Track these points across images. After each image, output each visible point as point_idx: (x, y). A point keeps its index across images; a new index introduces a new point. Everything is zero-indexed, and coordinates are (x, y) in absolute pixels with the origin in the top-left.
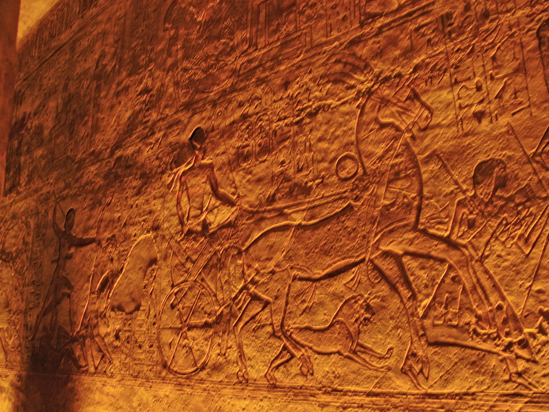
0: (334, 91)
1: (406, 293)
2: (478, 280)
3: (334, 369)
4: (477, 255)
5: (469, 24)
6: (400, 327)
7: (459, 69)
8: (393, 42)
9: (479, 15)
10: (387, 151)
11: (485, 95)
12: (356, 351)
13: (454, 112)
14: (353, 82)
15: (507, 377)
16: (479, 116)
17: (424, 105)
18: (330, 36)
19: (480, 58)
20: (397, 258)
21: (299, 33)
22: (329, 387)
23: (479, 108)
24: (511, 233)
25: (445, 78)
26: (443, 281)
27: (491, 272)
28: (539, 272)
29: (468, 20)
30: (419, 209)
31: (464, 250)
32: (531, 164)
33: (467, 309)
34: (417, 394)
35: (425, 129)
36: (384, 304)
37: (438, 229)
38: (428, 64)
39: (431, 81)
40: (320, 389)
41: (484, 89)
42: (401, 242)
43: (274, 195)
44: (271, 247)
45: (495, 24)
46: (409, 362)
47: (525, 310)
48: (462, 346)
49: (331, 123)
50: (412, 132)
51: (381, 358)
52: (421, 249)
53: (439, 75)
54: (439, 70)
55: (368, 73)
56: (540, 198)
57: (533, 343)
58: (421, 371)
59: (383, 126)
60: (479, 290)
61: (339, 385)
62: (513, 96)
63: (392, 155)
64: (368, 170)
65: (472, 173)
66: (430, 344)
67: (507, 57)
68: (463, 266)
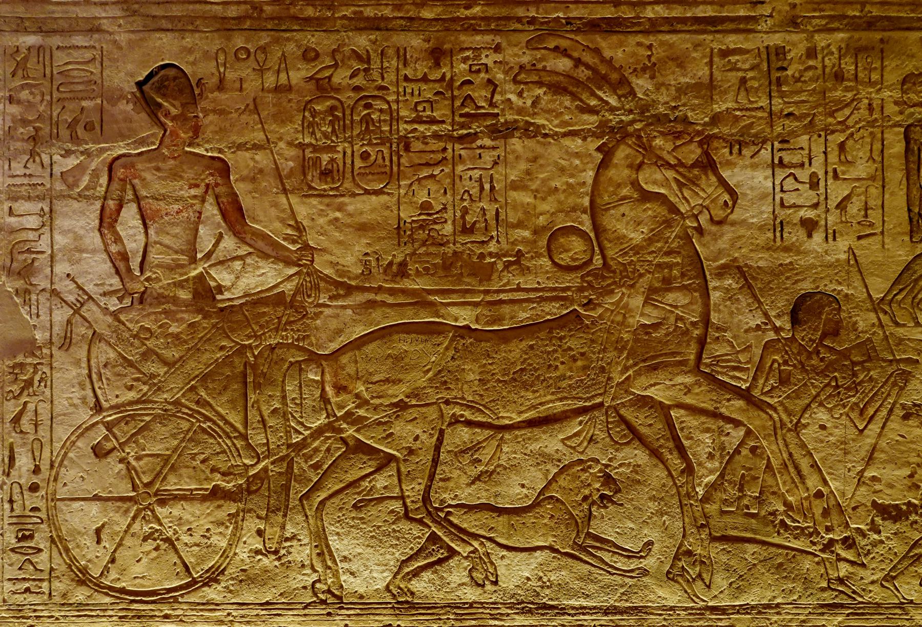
1: (675, 462)
2: (791, 455)
3: (541, 574)
4: (791, 422)
6: (666, 514)
7: (786, 146)
8: (680, 61)
10: (650, 241)
11: (822, 198)
12: (585, 546)
14: (593, 102)
15: (824, 584)
16: (809, 226)
17: (723, 182)
19: (822, 140)
20: (663, 410)
22: (532, 603)
24: (842, 400)
25: (763, 151)
26: (737, 451)
28: (875, 455)
30: (702, 343)
31: (771, 412)
32: (877, 313)
33: (774, 493)
34: (692, 608)
35: (720, 223)
36: (638, 477)
37: (732, 377)
38: (737, 119)
39: (740, 150)
40: (511, 606)
41: (822, 190)
43: (403, 265)
44: (398, 359)
45: (850, 95)
46: (680, 564)
47: (853, 501)
49: (542, 162)
51: (631, 555)
53: (754, 144)
58: (699, 575)
59: (646, 196)
60: (792, 470)
63: (660, 249)
66: (714, 539)
67: (861, 154)
68: (770, 435)
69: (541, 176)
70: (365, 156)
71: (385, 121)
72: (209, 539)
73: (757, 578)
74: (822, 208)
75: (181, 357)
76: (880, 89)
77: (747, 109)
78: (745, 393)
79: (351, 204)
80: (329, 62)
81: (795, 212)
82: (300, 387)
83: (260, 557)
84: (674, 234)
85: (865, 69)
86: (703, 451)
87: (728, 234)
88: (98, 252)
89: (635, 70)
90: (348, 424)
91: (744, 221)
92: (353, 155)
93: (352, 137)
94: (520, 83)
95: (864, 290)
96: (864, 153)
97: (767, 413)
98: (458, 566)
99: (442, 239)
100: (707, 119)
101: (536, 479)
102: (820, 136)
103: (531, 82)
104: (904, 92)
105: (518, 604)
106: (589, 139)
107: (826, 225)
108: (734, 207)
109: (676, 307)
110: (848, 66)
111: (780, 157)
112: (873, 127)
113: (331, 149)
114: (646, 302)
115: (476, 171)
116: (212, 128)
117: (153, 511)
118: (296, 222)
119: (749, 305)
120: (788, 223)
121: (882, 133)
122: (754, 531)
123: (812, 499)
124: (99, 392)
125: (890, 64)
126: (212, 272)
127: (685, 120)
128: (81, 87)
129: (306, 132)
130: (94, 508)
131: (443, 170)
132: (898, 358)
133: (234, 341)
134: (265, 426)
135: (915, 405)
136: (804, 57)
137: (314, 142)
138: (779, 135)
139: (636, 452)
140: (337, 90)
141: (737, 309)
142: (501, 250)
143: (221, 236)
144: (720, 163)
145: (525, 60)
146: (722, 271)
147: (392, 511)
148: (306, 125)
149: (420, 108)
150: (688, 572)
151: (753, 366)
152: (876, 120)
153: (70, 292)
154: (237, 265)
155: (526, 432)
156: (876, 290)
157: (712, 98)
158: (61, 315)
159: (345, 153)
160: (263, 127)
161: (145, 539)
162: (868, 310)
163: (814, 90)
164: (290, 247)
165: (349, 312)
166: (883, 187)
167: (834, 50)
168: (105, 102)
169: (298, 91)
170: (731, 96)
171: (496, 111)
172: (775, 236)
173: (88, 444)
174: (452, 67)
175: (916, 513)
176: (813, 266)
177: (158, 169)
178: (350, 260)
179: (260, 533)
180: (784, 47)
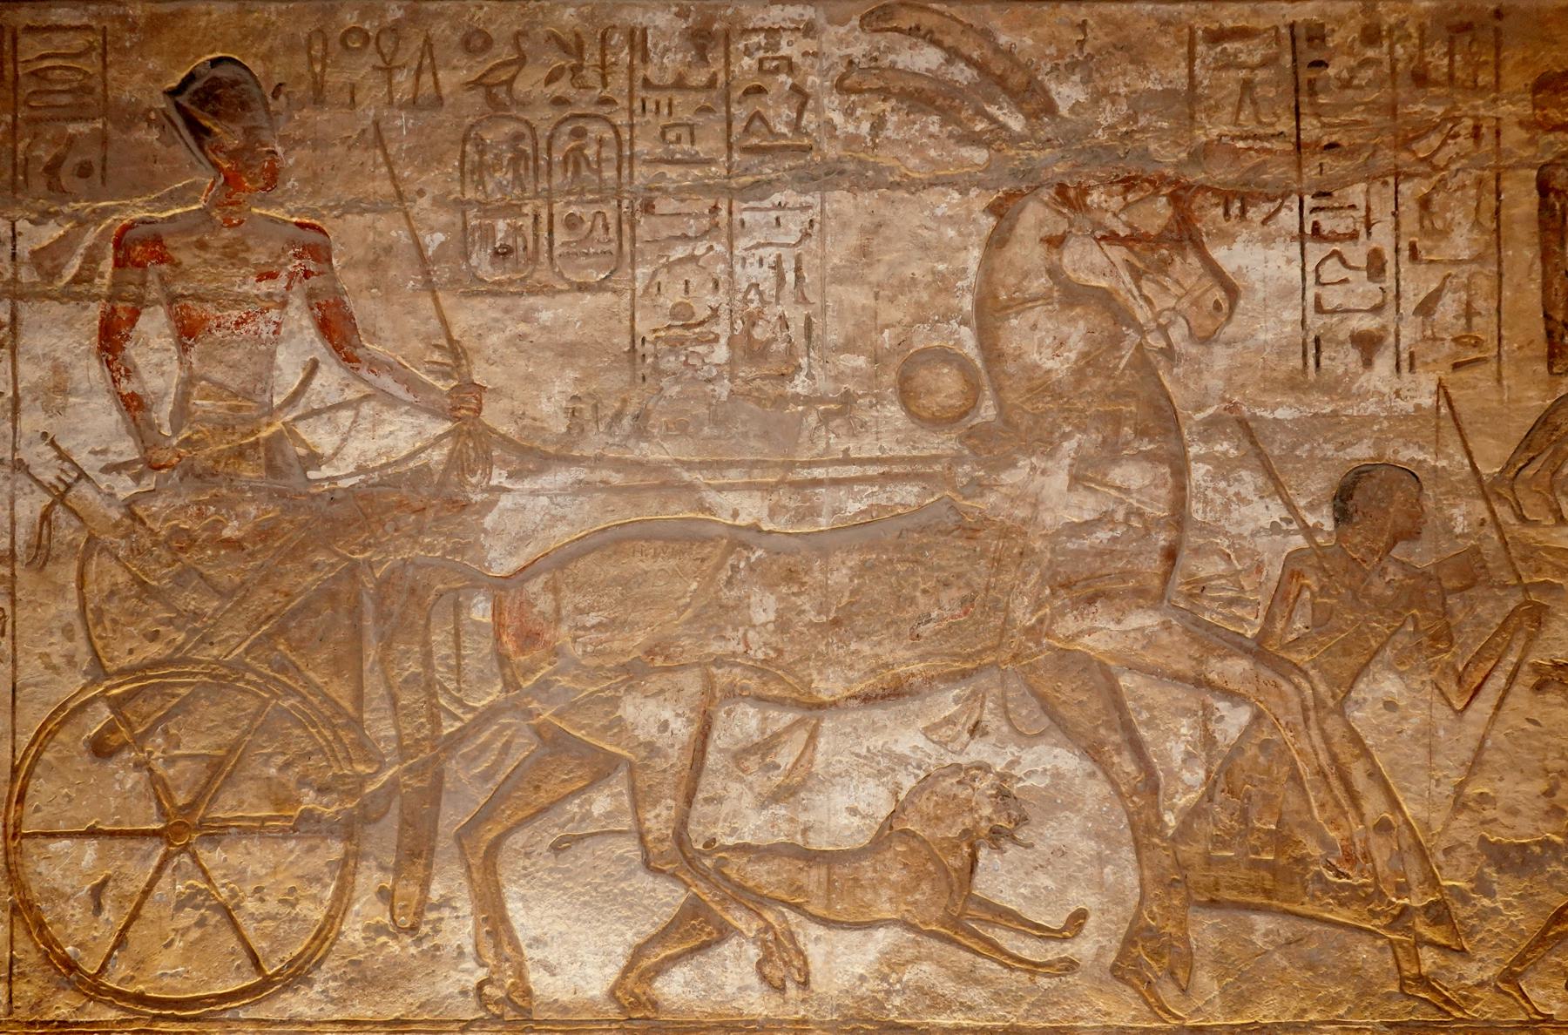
2: (1334, 758)
3: (886, 970)
7: (1324, 202)
11: (1391, 296)
13: (1298, 316)
16: (1367, 344)
23: (1368, 323)
25: (1284, 212)
26: (1238, 748)
27: (1369, 742)
28: (1486, 756)
29: (1370, 73)
32: (1487, 500)
33: (1302, 825)
38: (1237, 153)
39: (1243, 211)
46: (1138, 951)
48: (1286, 912)
50: (1167, 339)
51: (1045, 934)
57: (1461, 911)
60: (1335, 782)
61: (904, 1015)
70: (572, 223)
71: (608, 160)
72: (293, 906)
73: (1273, 977)
74: (1390, 312)
75: (243, 583)
76: (1495, 101)
77: (1255, 137)
79: (547, 309)
80: (505, 53)
81: (1342, 321)
82: (457, 635)
83: (383, 939)
84: (1124, 362)
86: (1177, 750)
87: (1221, 358)
88: (96, 393)
89: (1056, 67)
90: (540, 702)
92: (551, 222)
93: (549, 190)
94: (850, 91)
95: (1466, 461)
96: (1466, 216)
97: (1290, 681)
98: (738, 958)
99: (710, 371)
101: (876, 800)
102: (1385, 183)
103: (870, 90)
105: (844, 1023)
106: (973, 192)
107: (1397, 346)
108: (1232, 308)
109: (1127, 491)
110: (1437, 59)
111: (1315, 223)
113: (512, 209)
115: (770, 250)
116: (300, 172)
117: (194, 856)
118: (450, 339)
119: (1256, 489)
121: (1498, 179)
122: (1268, 893)
123: (1371, 835)
124: (99, 644)
125: (1512, 55)
126: (301, 429)
128: (65, 99)
129: (468, 180)
130: (90, 851)
131: (711, 248)
133: (337, 554)
134: (394, 704)
135: (1557, 666)
136: (1357, 45)
137: (480, 196)
139: (1057, 751)
140: (523, 104)
142: (815, 391)
143: (313, 367)
144: (1208, 234)
145: (858, 51)
146: (1212, 428)
147: (621, 858)
148: (467, 166)
149: (671, 136)
150: (1150, 968)
153: (46, 465)
154: (345, 416)
155: (862, 716)
157: (1192, 117)
158: (30, 506)
159: (536, 217)
160: (391, 170)
161: (180, 906)
162: (1472, 497)
163: (1373, 102)
164: (439, 384)
165: (544, 500)
167: (1412, 30)
168: (110, 127)
169: (453, 105)
171: (806, 141)
172: (1305, 364)
173: (79, 738)
174: (728, 63)
175: (1558, 860)
176: (1374, 418)
177: (202, 245)
178: (549, 408)
179: (385, 895)
180: (1322, 26)
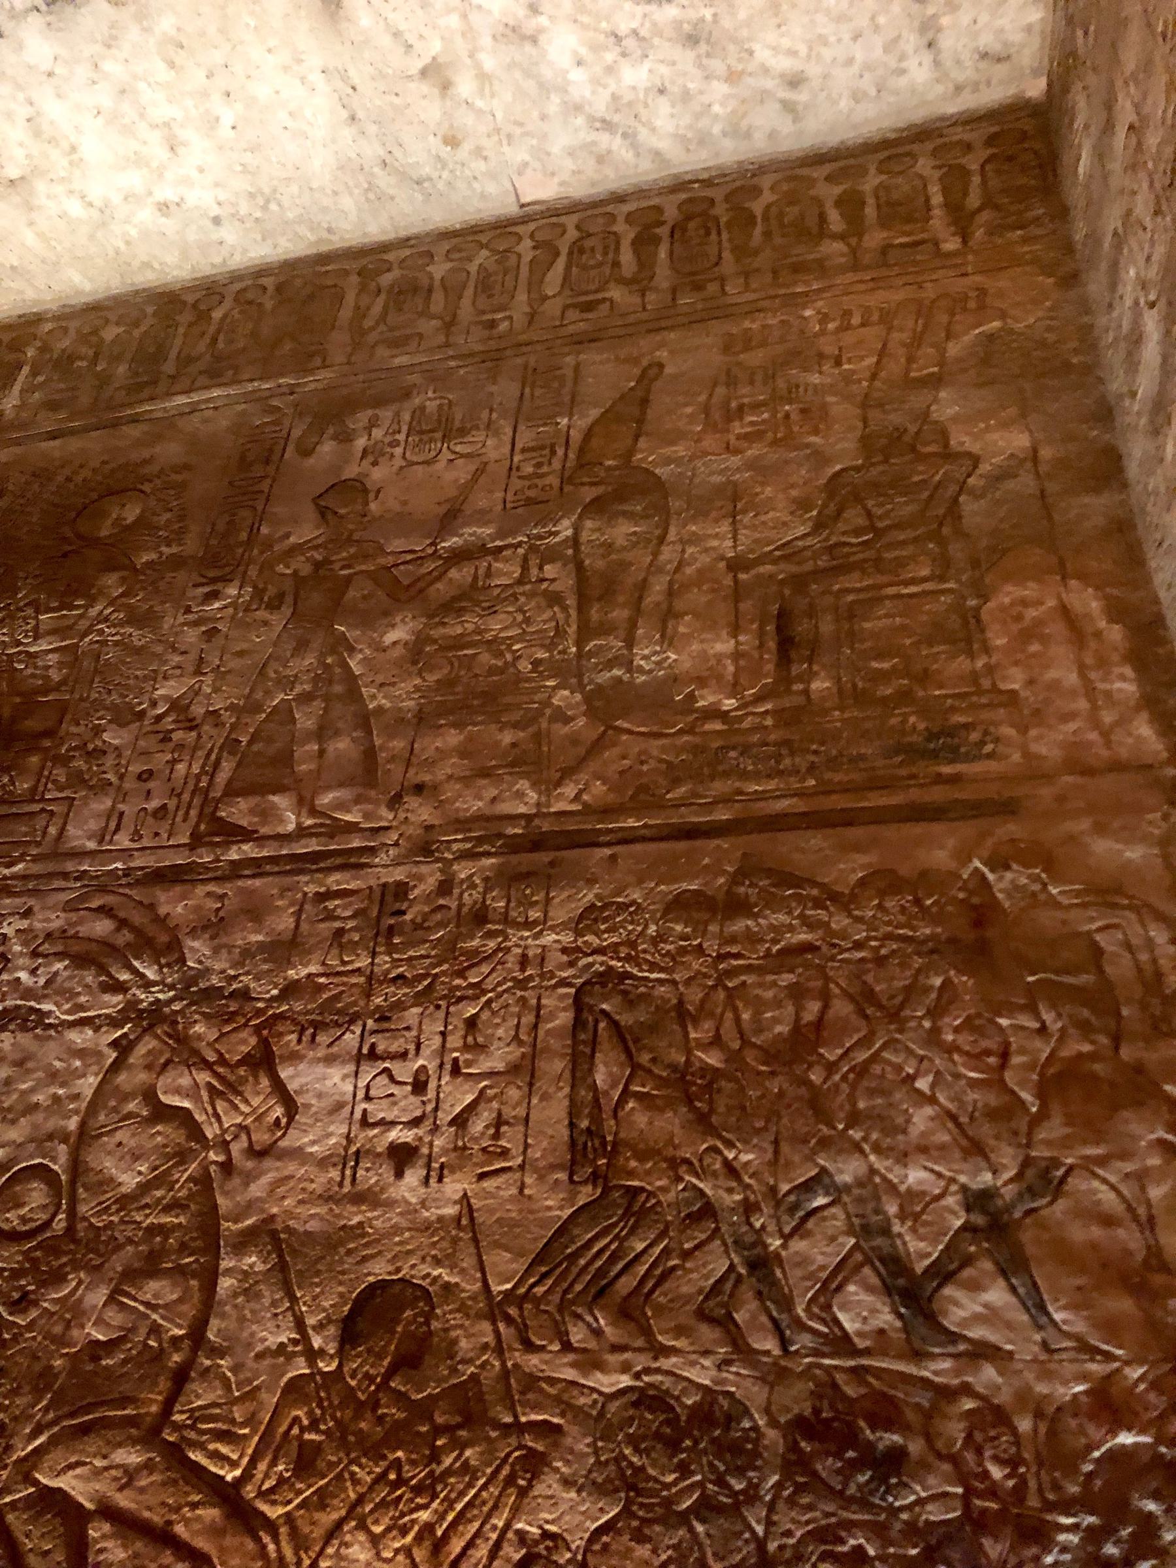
0: (67, 985)
5: (441, 925)
7: (386, 1025)
8: (255, 912)
9: (465, 910)
10: (144, 1188)
11: (430, 1107)
13: (344, 1129)
14: (124, 976)
16: (401, 1156)
17: (280, 1089)
18: (111, 842)
19: (441, 1014)
21: (36, 807)
24: (403, 1515)
25: (348, 1036)
31: (266, 1539)
32: (494, 1323)
38: (321, 988)
39: (314, 1036)
41: (431, 1094)
42: (98, 1473)
45: (492, 944)
52: (149, 1509)
53: (337, 1025)
54: (339, 1012)
55: (168, 965)
56: (498, 1425)
59: (161, 1113)
62: (492, 1131)
64: (81, 1226)
65: (347, 1308)
67: (500, 1032)
69: (24, 1086)
74: (427, 1124)
77: (338, 974)
78: (231, 1491)
85: (520, 904)
87: (272, 1171)
91: (300, 1148)
100: (275, 992)
102: (438, 1007)
104: (579, 933)
112: (525, 989)
114: (111, 1299)
119: (274, 1304)
120: (368, 1152)
127: (244, 995)
132: (523, 1419)
135: (546, 1535)
138: (378, 1007)
141: (253, 1312)
146: (244, 1242)
151: (254, 1431)
152: (531, 978)
156: (499, 1274)
166: (531, 1085)
170: (317, 956)
176: (396, 1230)
